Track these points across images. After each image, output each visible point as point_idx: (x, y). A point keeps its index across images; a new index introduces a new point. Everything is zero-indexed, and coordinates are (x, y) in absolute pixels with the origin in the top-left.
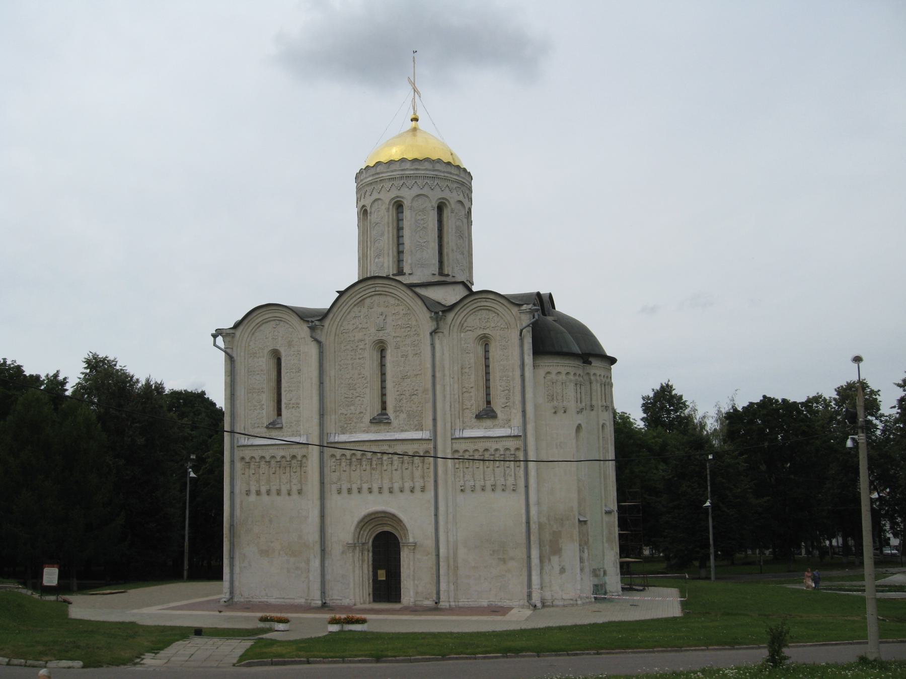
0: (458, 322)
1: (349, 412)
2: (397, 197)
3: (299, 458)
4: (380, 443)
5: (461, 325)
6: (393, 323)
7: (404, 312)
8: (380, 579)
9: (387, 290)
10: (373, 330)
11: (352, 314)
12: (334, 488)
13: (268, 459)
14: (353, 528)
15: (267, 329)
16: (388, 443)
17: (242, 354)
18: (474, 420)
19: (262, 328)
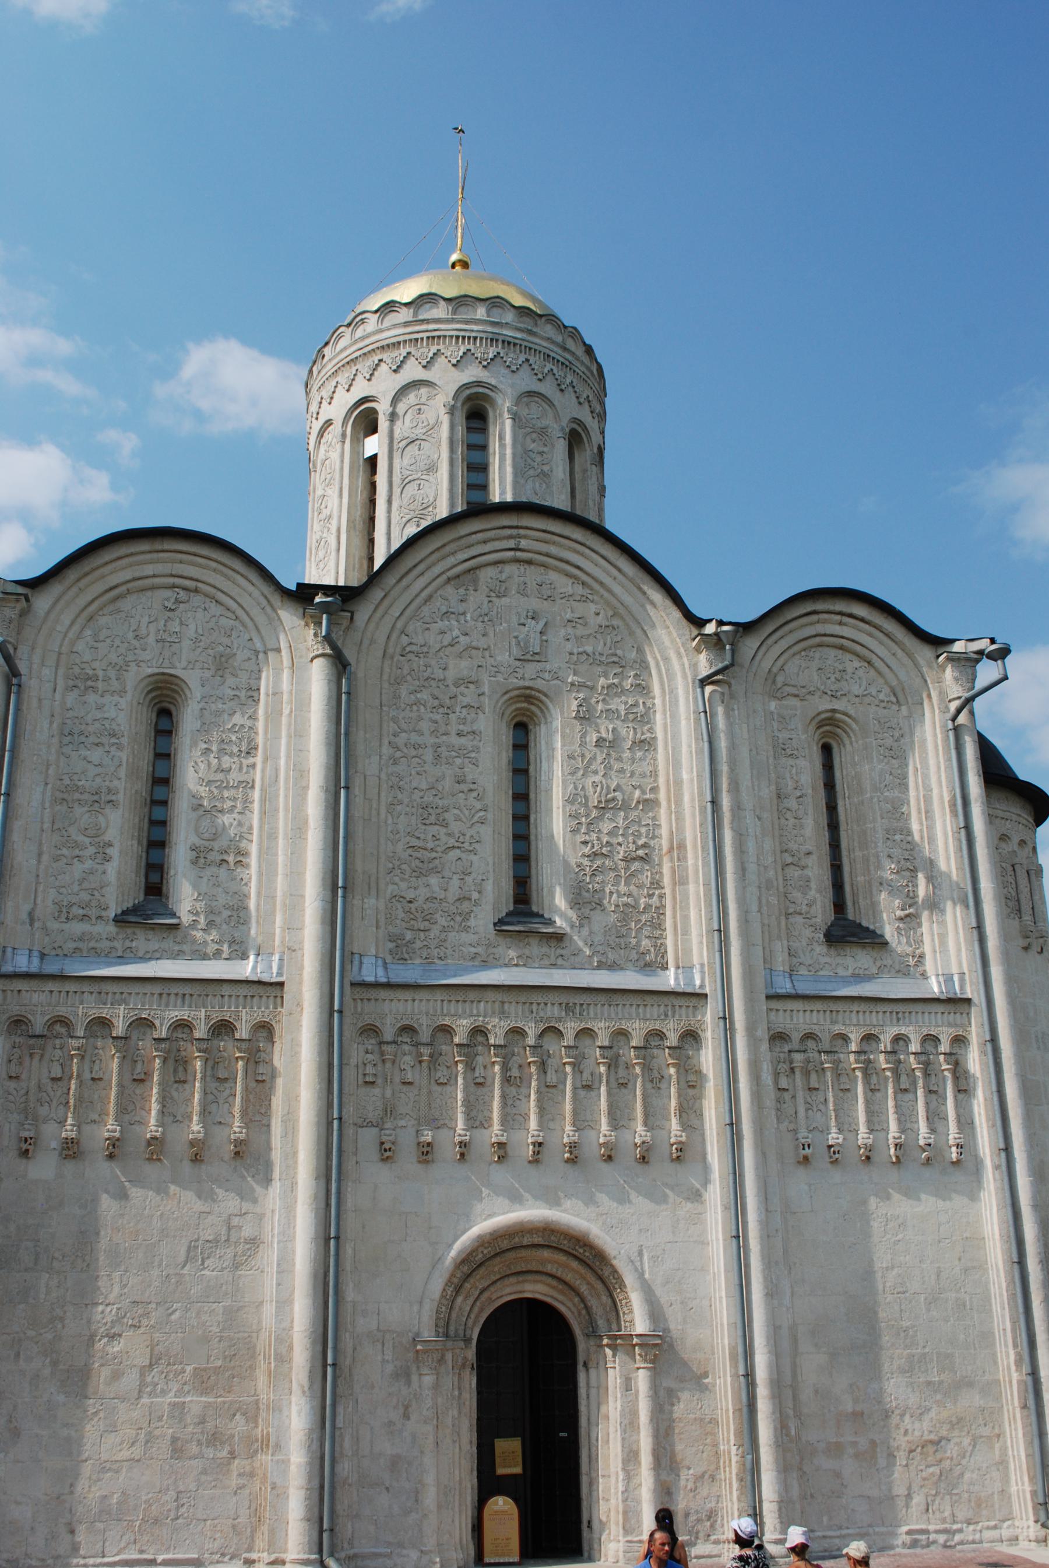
0: (767, 664)
1: (423, 893)
2: (479, 384)
3: (243, 1031)
4: (537, 997)
5: (771, 677)
6: (569, 646)
7: (601, 620)
8: (501, 1471)
9: (553, 550)
10: (503, 657)
11: (438, 603)
12: (368, 1137)
13: (120, 1028)
14: (437, 1286)
15: (143, 612)
16: (564, 998)
17: (46, 672)
18: (820, 949)
19: (126, 604)
